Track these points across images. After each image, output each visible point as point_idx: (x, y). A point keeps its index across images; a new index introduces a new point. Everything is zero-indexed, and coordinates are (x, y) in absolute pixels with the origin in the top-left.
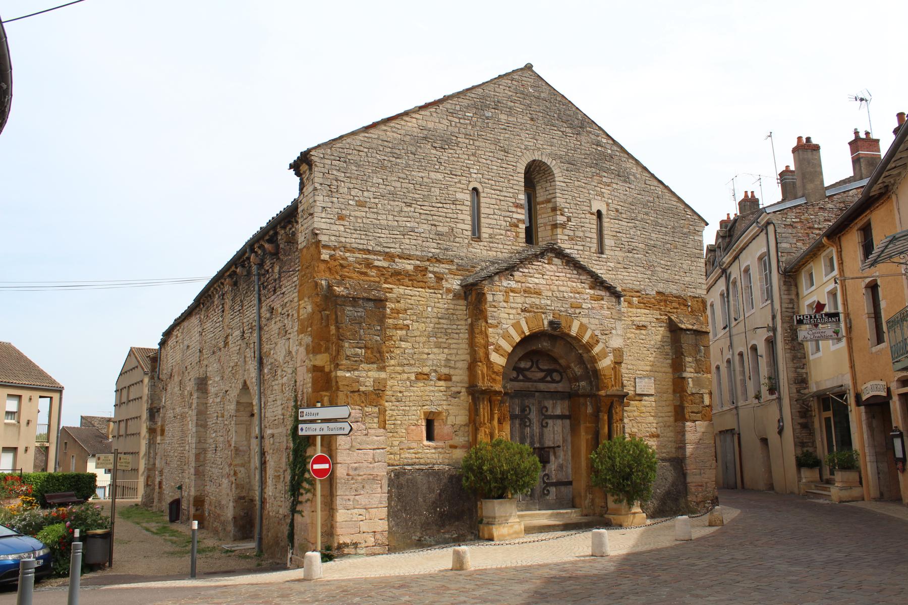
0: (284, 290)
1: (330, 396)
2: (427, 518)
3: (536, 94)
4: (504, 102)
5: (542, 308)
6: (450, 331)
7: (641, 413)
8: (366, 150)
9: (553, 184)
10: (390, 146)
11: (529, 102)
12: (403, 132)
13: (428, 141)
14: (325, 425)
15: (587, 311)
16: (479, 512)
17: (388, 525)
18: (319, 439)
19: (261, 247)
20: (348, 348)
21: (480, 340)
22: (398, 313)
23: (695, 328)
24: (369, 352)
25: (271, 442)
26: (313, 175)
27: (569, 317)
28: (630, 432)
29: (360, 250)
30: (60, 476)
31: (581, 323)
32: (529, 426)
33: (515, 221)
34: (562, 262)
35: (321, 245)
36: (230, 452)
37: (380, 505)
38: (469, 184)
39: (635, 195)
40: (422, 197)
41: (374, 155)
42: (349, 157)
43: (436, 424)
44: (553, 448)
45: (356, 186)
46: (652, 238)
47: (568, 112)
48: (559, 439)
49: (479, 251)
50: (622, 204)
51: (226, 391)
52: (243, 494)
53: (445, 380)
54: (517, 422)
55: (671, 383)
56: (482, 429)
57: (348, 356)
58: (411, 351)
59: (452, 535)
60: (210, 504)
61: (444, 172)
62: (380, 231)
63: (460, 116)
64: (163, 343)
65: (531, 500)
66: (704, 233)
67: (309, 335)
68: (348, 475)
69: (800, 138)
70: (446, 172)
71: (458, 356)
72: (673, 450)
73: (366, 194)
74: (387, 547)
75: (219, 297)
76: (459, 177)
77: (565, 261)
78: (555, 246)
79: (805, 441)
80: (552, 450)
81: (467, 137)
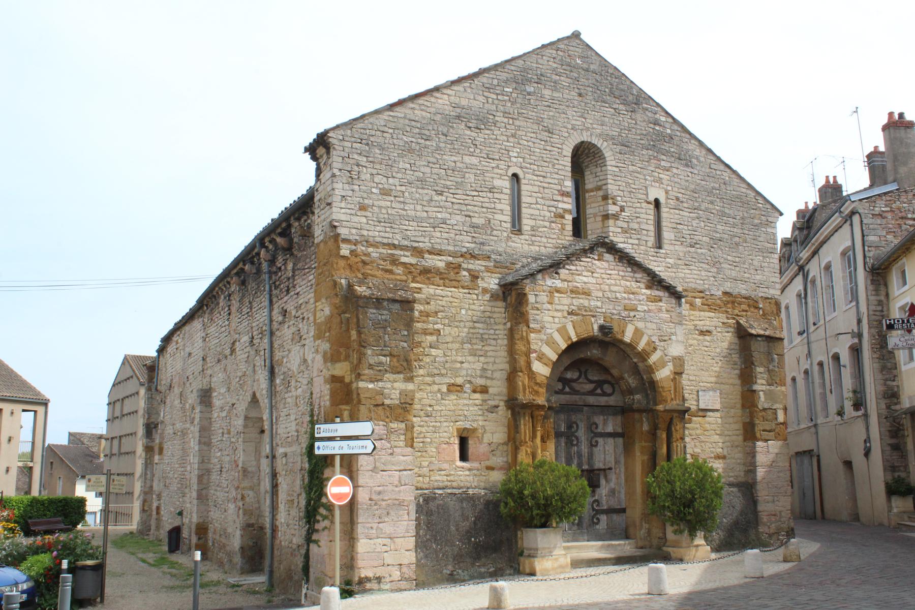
0: (299, 290)
1: (351, 410)
2: (460, 549)
3: (585, 66)
4: (548, 75)
5: (591, 311)
6: (486, 337)
7: (705, 431)
8: (391, 131)
9: (603, 168)
10: (419, 125)
11: (576, 75)
12: (433, 110)
13: (462, 121)
14: (344, 443)
16: (520, 542)
17: (416, 557)
18: (338, 460)
19: (273, 241)
20: (371, 356)
21: (520, 347)
22: (428, 315)
23: (767, 333)
24: (395, 360)
25: (284, 462)
26: (331, 160)
27: (623, 321)
28: (692, 453)
29: (384, 244)
30: (46, 500)
31: (637, 330)
32: (577, 445)
33: (561, 211)
34: (615, 258)
35: (340, 239)
36: (237, 474)
37: (407, 535)
38: (508, 169)
39: (698, 181)
40: (454, 184)
41: (400, 136)
42: (372, 139)
43: (470, 442)
44: (604, 470)
45: (380, 172)
46: (718, 230)
47: (621, 86)
48: (611, 460)
49: (520, 245)
50: (683, 191)
51: (233, 405)
52: (251, 522)
53: (481, 392)
54: (563, 441)
55: (739, 397)
56: (523, 448)
57: (370, 365)
58: (443, 359)
59: (488, 569)
60: (215, 533)
61: (480, 155)
62: (407, 223)
63: (498, 92)
64: (161, 350)
65: (579, 529)
66: (778, 224)
67: (327, 341)
68: (371, 499)
69: (891, 114)
70: (482, 155)
71: (495, 365)
72: (742, 474)
73: (391, 181)
74: (414, 582)
75: (225, 298)
76: (497, 162)
77: (617, 257)
78: (606, 240)
79: (896, 464)
80: (602, 473)
81: (506, 115)
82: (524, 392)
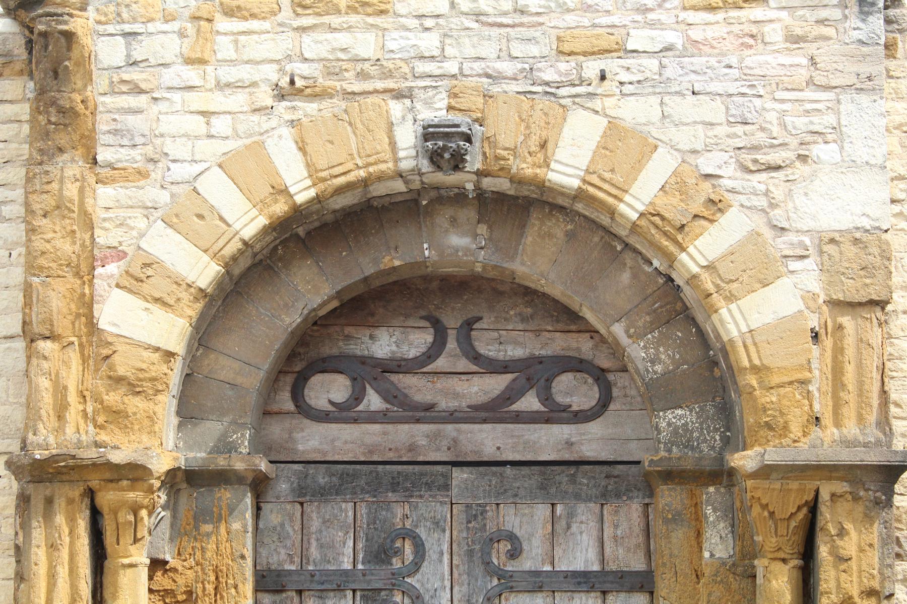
5: (388, 74)
15: (653, 64)
31: (614, 128)
82: (60, 417)
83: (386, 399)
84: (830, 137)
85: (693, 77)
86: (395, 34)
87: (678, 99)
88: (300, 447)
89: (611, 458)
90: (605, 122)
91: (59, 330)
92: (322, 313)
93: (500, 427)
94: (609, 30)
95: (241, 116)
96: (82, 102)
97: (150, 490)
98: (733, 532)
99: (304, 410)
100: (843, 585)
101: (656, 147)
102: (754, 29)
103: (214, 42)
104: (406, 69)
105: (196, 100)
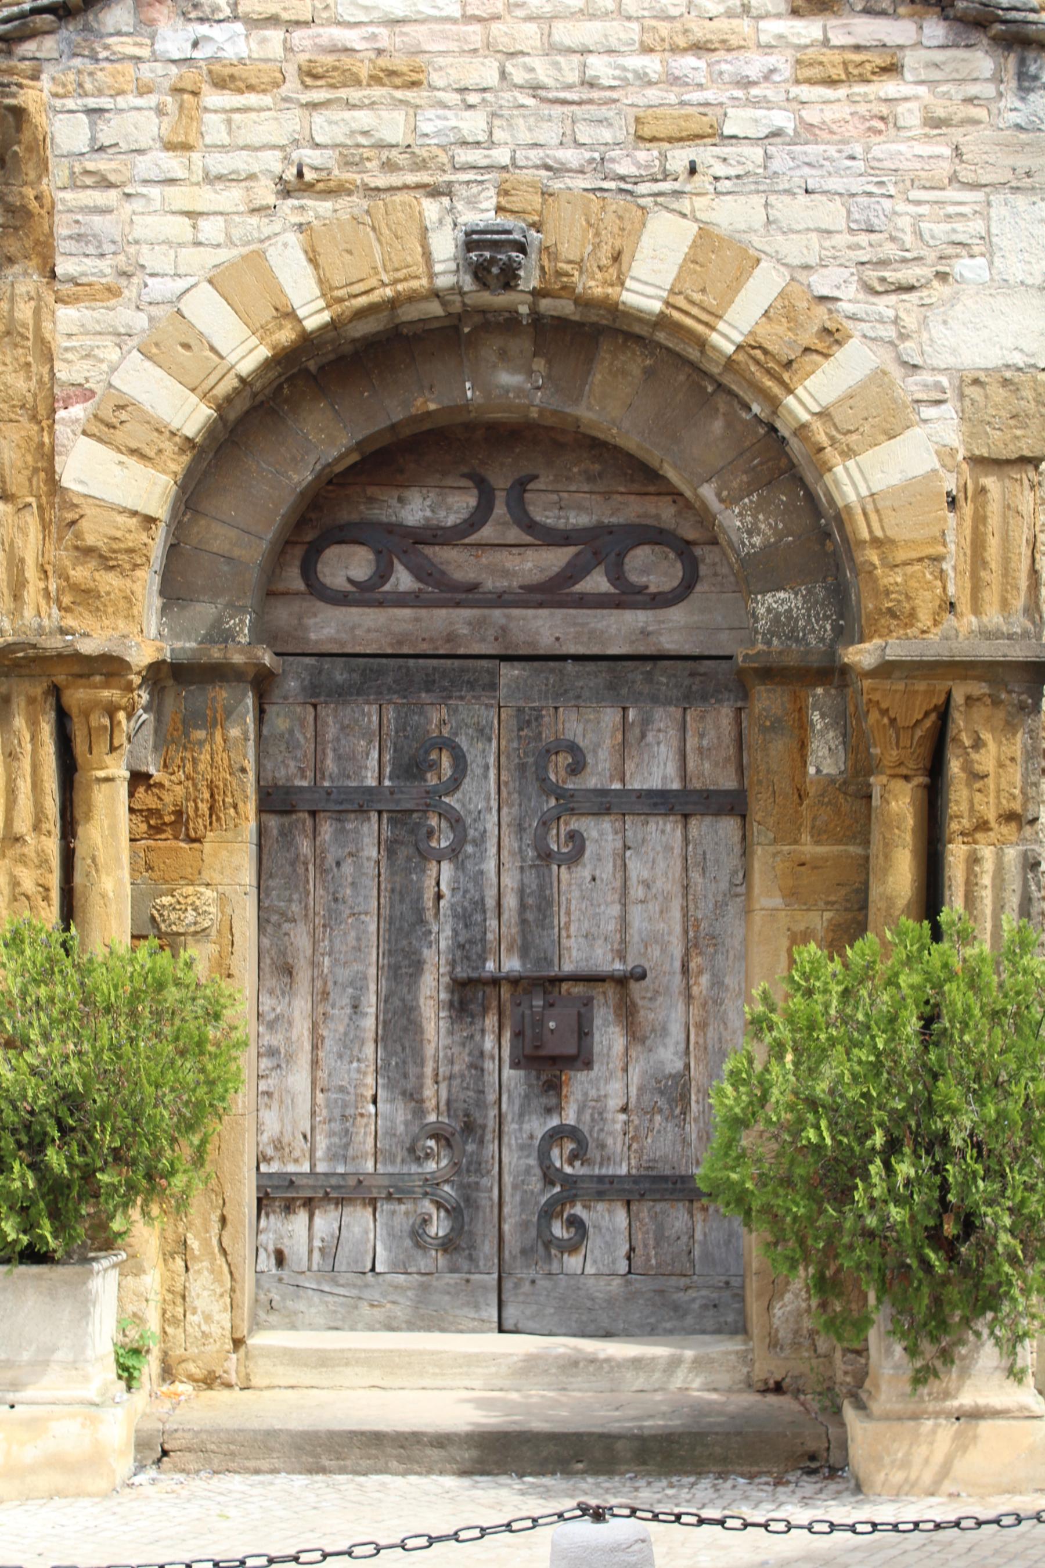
5: (421, 165)
15: (756, 153)
32: (454, 853)
44: (621, 981)
65: (452, 1271)
82: (17, 597)
83: (418, 578)
84: (976, 250)
85: (806, 170)
86: (431, 113)
87: (787, 199)
88: (313, 636)
89: (697, 651)
90: (695, 227)
91: (13, 489)
92: (339, 468)
93: (560, 613)
94: (702, 110)
95: (236, 218)
96: (36, 198)
97: (129, 688)
98: (844, 743)
99: (317, 591)
100: (977, 807)
101: (758, 261)
102: (884, 110)
103: (201, 121)
104: (443, 158)
105: (180, 197)
